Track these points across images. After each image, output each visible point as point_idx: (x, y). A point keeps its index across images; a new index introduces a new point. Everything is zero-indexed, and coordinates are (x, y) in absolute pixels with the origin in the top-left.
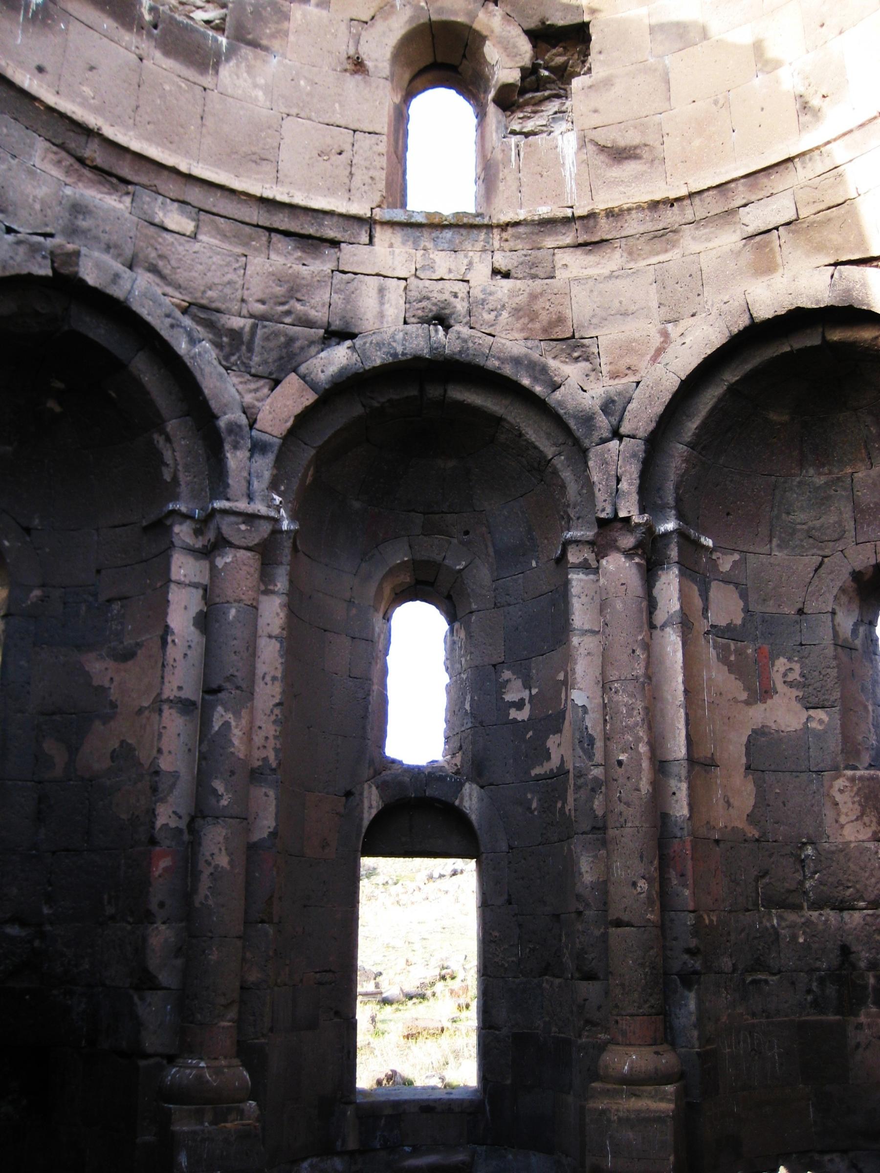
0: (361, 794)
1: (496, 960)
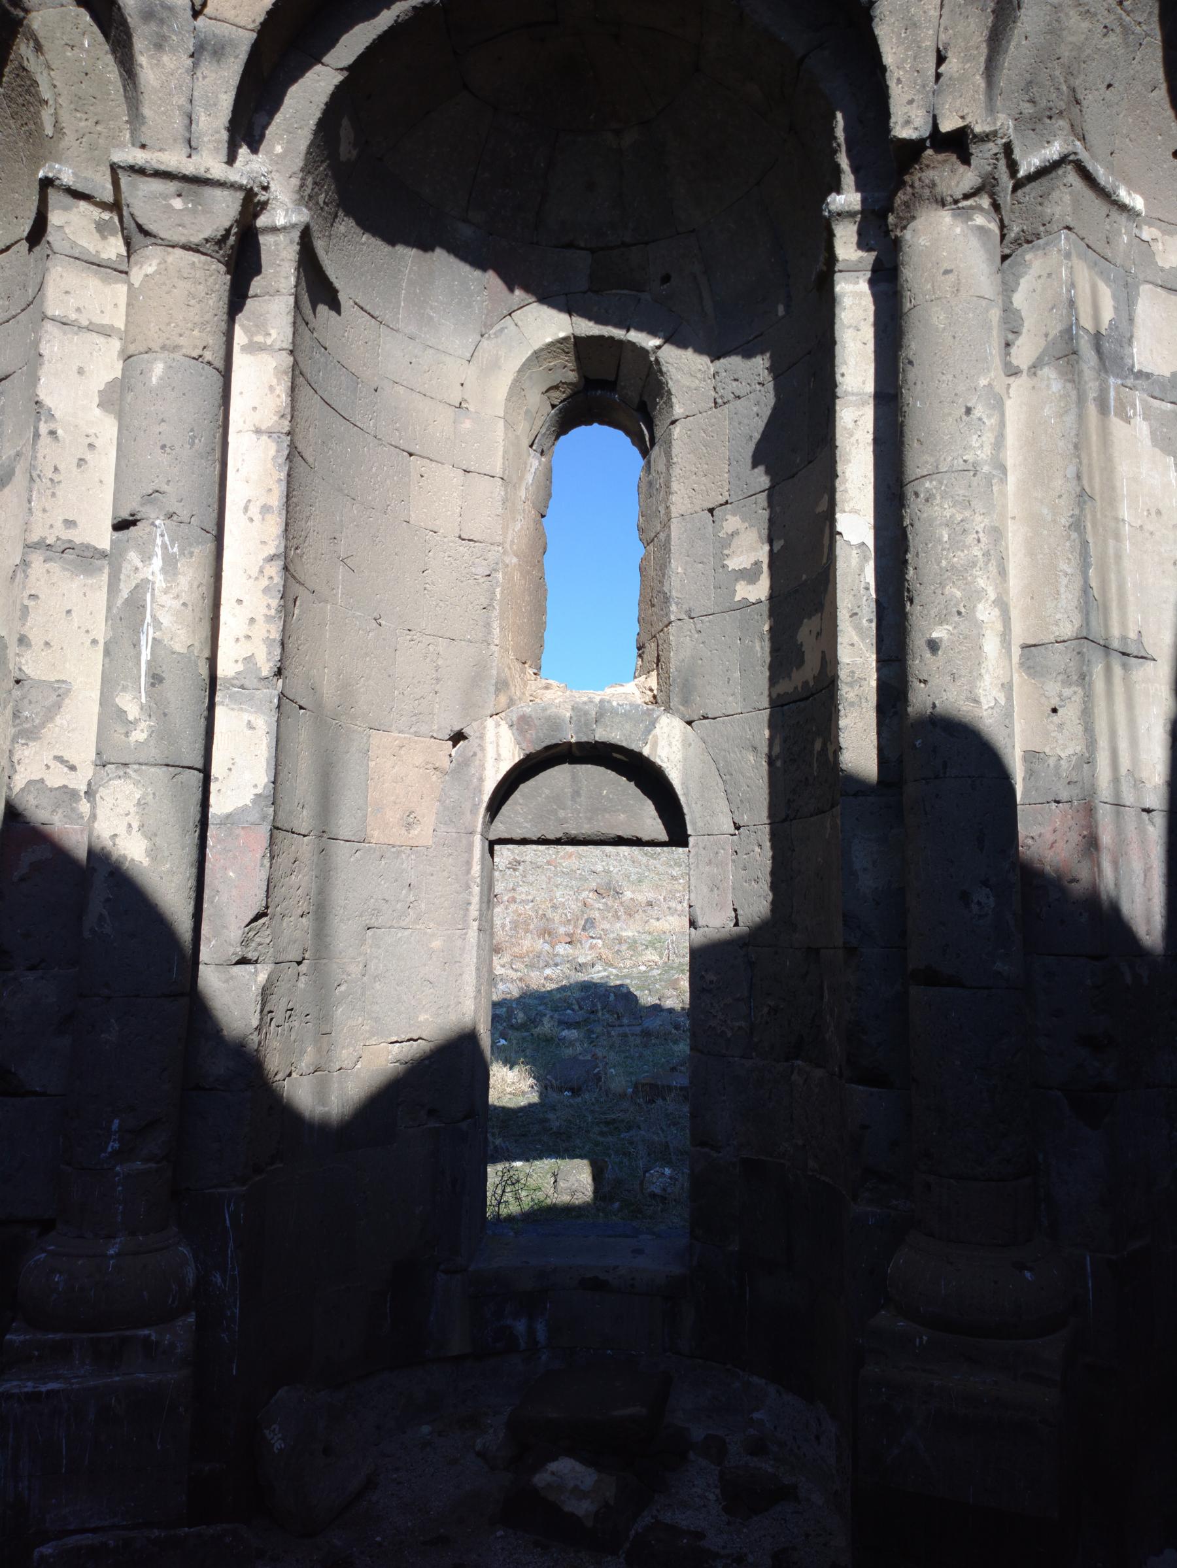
0: (482, 737)
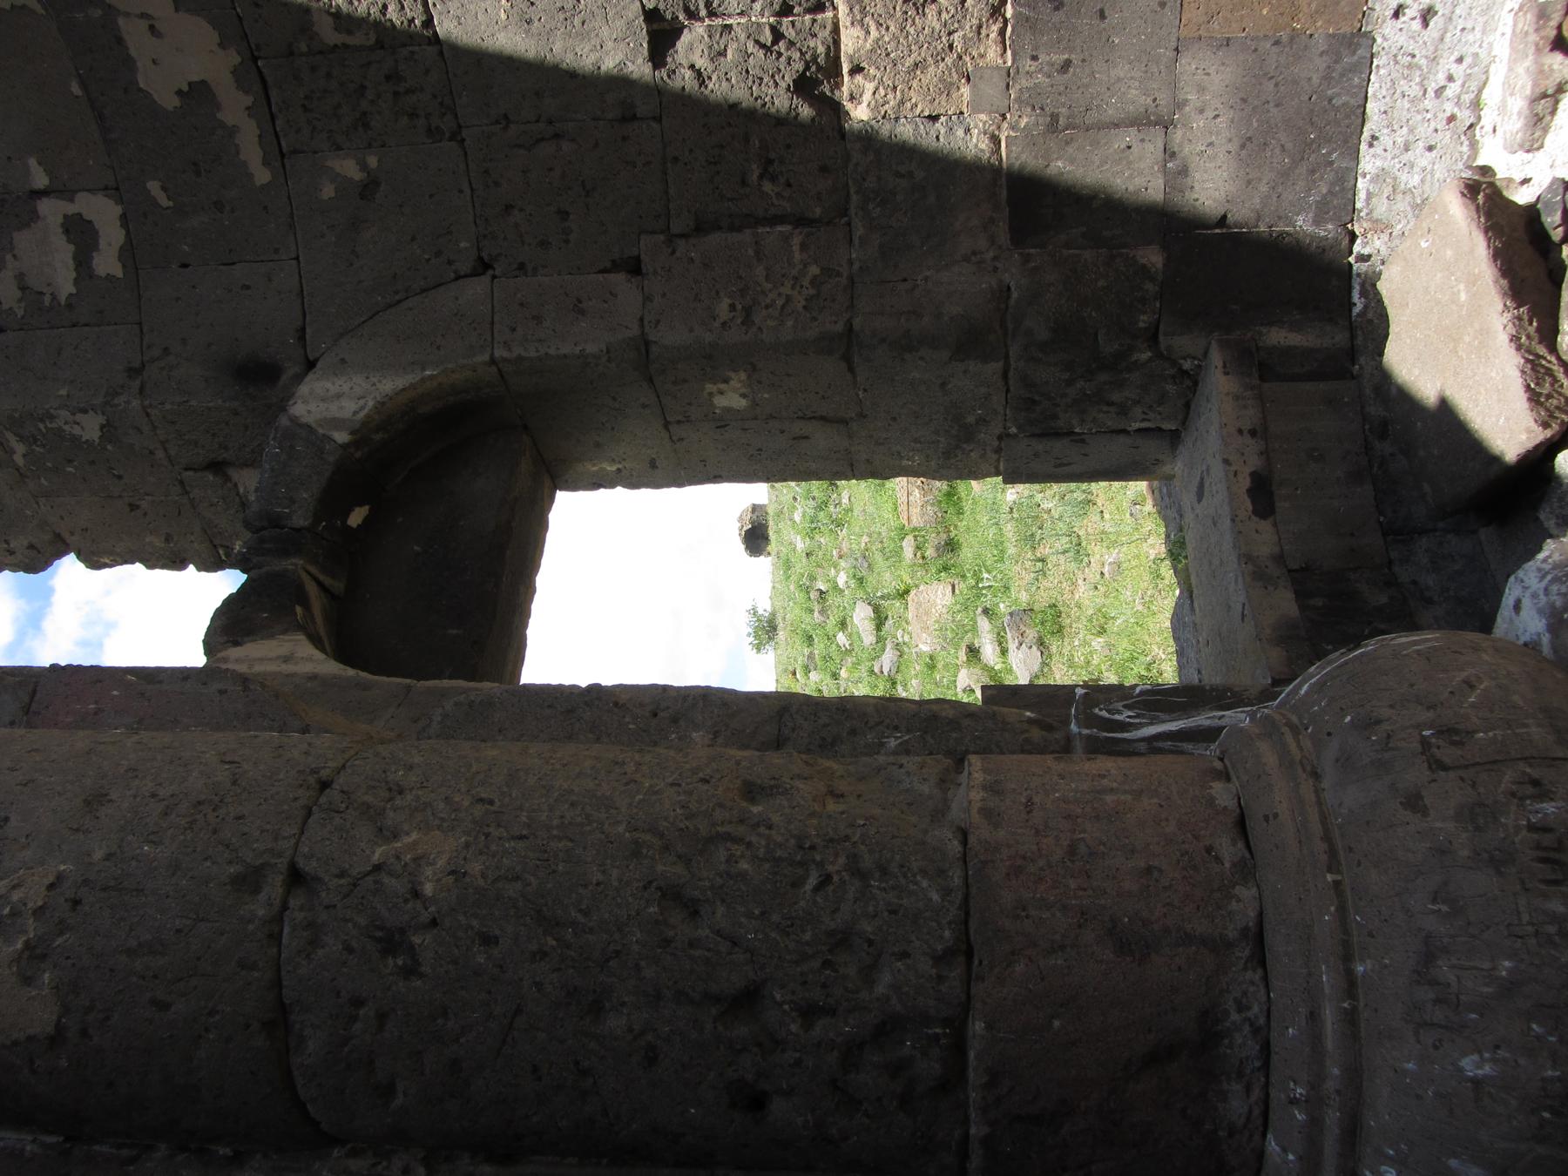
1: (800, 303)
